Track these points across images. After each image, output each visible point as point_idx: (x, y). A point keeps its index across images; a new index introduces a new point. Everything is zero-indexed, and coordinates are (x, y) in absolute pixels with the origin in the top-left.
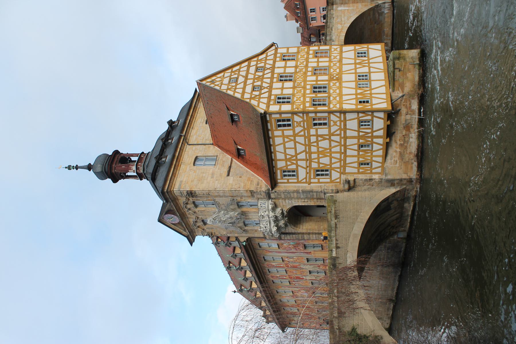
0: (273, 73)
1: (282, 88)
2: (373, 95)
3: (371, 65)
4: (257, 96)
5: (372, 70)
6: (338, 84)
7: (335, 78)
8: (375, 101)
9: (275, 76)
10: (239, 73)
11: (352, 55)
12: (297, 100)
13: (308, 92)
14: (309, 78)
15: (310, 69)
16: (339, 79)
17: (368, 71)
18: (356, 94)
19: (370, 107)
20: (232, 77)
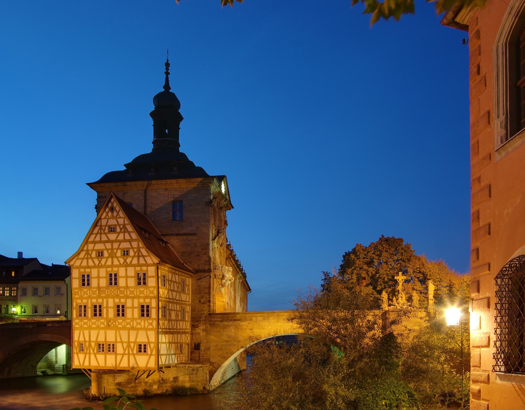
0: (120, 265)
1: (98, 277)
2: (88, 355)
3: (126, 358)
4: (91, 255)
5: (119, 358)
6: (102, 326)
7: (110, 323)
8: (82, 356)
9: (115, 269)
10: (122, 232)
11: (142, 339)
12: (84, 292)
13: (94, 301)
14: (111, 301)
15: (123, 300)
16: (108, 327)
17: (118, 352)
18: (90, 341)
19: (75, 352)
20: (118, 227)
